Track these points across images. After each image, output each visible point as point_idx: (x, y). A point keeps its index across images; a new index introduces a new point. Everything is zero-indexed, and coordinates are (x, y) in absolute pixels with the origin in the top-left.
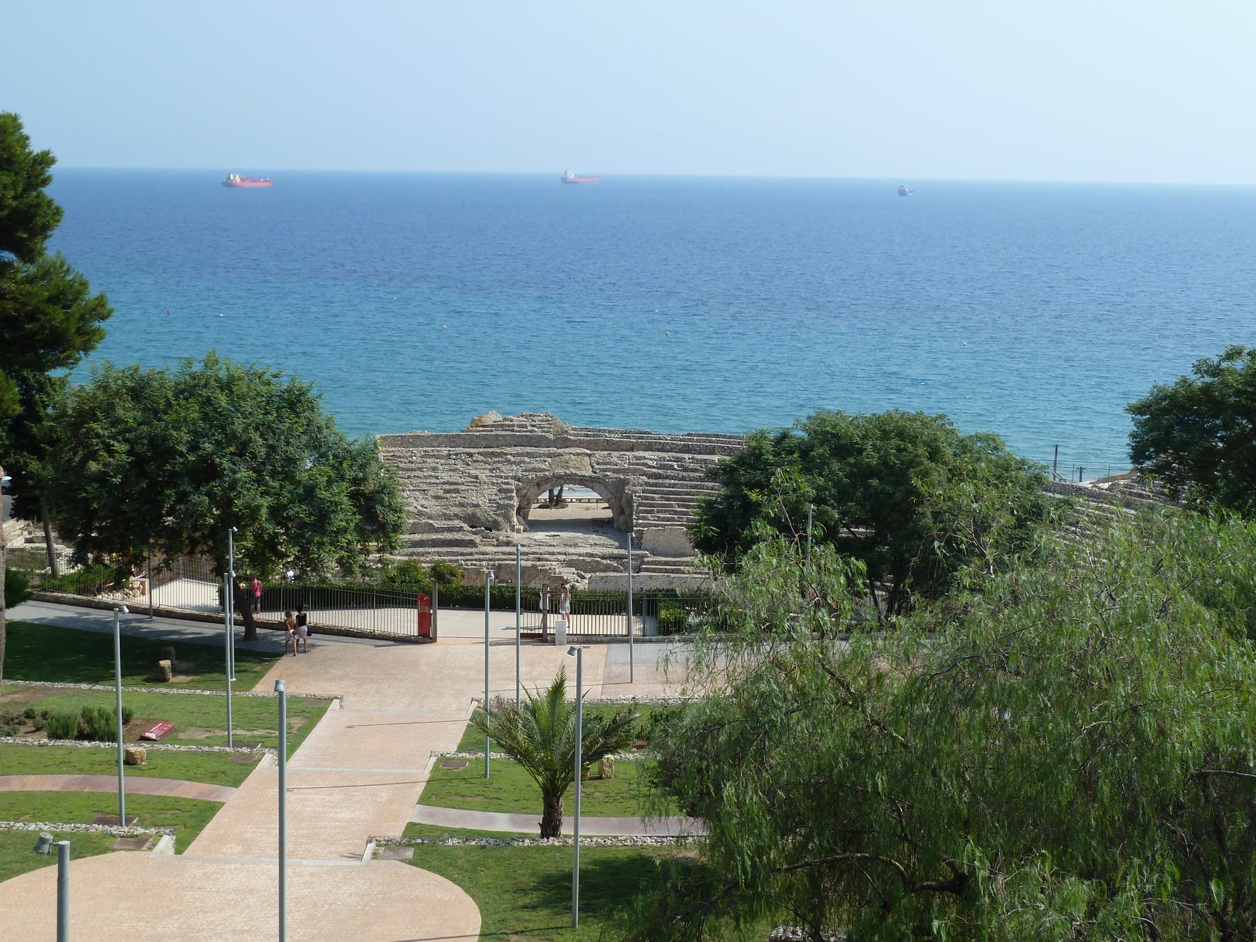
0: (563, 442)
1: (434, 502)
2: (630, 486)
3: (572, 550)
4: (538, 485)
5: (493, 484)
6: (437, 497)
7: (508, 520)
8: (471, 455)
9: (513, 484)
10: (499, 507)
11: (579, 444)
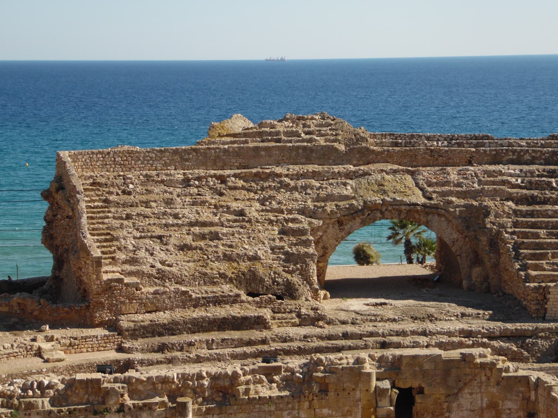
0: (360, 154)
1: (181, 256)
2: (492, 218)
3: (430, 326)
4: (340, 223)
5: (271, 222)
6: (184, 248)
7: (307, 279)
8: (223, 180)
9: (305, 223)
10: (289, 258)
11: (386, 157)
